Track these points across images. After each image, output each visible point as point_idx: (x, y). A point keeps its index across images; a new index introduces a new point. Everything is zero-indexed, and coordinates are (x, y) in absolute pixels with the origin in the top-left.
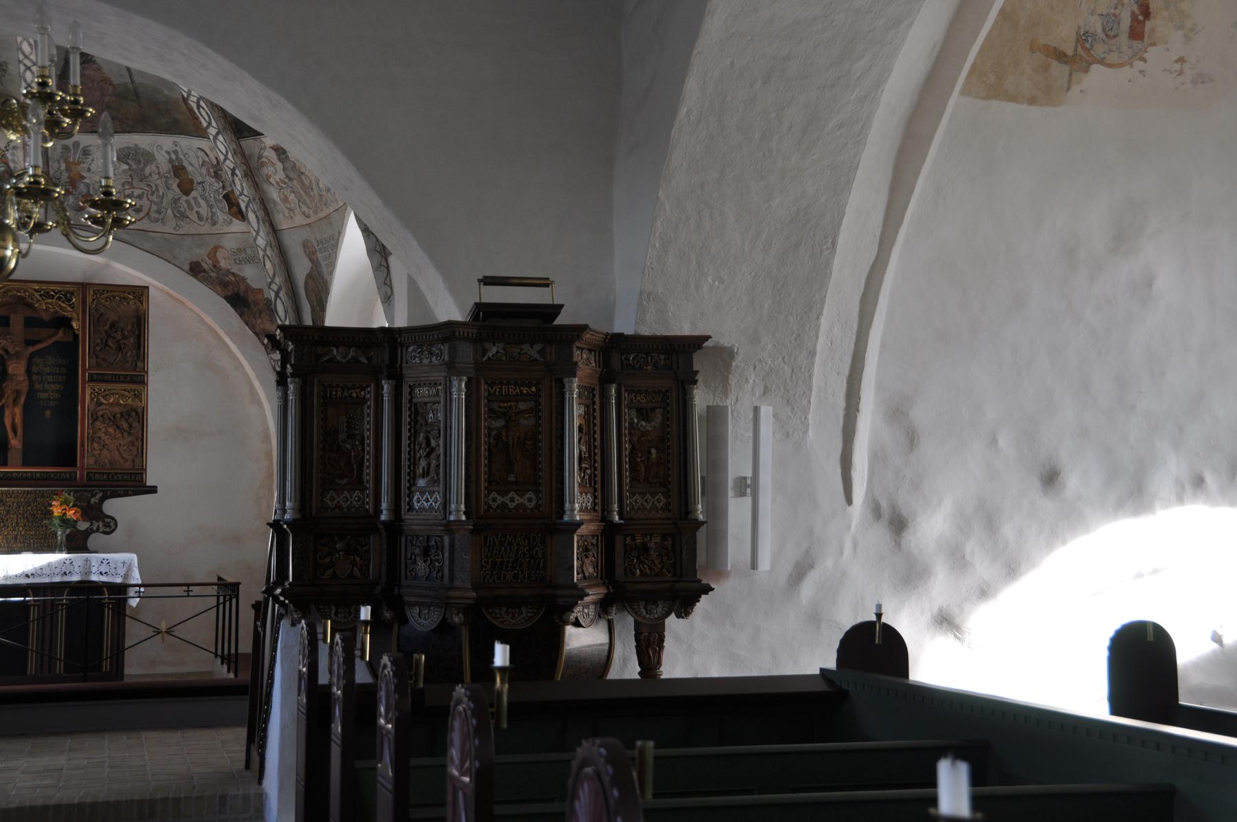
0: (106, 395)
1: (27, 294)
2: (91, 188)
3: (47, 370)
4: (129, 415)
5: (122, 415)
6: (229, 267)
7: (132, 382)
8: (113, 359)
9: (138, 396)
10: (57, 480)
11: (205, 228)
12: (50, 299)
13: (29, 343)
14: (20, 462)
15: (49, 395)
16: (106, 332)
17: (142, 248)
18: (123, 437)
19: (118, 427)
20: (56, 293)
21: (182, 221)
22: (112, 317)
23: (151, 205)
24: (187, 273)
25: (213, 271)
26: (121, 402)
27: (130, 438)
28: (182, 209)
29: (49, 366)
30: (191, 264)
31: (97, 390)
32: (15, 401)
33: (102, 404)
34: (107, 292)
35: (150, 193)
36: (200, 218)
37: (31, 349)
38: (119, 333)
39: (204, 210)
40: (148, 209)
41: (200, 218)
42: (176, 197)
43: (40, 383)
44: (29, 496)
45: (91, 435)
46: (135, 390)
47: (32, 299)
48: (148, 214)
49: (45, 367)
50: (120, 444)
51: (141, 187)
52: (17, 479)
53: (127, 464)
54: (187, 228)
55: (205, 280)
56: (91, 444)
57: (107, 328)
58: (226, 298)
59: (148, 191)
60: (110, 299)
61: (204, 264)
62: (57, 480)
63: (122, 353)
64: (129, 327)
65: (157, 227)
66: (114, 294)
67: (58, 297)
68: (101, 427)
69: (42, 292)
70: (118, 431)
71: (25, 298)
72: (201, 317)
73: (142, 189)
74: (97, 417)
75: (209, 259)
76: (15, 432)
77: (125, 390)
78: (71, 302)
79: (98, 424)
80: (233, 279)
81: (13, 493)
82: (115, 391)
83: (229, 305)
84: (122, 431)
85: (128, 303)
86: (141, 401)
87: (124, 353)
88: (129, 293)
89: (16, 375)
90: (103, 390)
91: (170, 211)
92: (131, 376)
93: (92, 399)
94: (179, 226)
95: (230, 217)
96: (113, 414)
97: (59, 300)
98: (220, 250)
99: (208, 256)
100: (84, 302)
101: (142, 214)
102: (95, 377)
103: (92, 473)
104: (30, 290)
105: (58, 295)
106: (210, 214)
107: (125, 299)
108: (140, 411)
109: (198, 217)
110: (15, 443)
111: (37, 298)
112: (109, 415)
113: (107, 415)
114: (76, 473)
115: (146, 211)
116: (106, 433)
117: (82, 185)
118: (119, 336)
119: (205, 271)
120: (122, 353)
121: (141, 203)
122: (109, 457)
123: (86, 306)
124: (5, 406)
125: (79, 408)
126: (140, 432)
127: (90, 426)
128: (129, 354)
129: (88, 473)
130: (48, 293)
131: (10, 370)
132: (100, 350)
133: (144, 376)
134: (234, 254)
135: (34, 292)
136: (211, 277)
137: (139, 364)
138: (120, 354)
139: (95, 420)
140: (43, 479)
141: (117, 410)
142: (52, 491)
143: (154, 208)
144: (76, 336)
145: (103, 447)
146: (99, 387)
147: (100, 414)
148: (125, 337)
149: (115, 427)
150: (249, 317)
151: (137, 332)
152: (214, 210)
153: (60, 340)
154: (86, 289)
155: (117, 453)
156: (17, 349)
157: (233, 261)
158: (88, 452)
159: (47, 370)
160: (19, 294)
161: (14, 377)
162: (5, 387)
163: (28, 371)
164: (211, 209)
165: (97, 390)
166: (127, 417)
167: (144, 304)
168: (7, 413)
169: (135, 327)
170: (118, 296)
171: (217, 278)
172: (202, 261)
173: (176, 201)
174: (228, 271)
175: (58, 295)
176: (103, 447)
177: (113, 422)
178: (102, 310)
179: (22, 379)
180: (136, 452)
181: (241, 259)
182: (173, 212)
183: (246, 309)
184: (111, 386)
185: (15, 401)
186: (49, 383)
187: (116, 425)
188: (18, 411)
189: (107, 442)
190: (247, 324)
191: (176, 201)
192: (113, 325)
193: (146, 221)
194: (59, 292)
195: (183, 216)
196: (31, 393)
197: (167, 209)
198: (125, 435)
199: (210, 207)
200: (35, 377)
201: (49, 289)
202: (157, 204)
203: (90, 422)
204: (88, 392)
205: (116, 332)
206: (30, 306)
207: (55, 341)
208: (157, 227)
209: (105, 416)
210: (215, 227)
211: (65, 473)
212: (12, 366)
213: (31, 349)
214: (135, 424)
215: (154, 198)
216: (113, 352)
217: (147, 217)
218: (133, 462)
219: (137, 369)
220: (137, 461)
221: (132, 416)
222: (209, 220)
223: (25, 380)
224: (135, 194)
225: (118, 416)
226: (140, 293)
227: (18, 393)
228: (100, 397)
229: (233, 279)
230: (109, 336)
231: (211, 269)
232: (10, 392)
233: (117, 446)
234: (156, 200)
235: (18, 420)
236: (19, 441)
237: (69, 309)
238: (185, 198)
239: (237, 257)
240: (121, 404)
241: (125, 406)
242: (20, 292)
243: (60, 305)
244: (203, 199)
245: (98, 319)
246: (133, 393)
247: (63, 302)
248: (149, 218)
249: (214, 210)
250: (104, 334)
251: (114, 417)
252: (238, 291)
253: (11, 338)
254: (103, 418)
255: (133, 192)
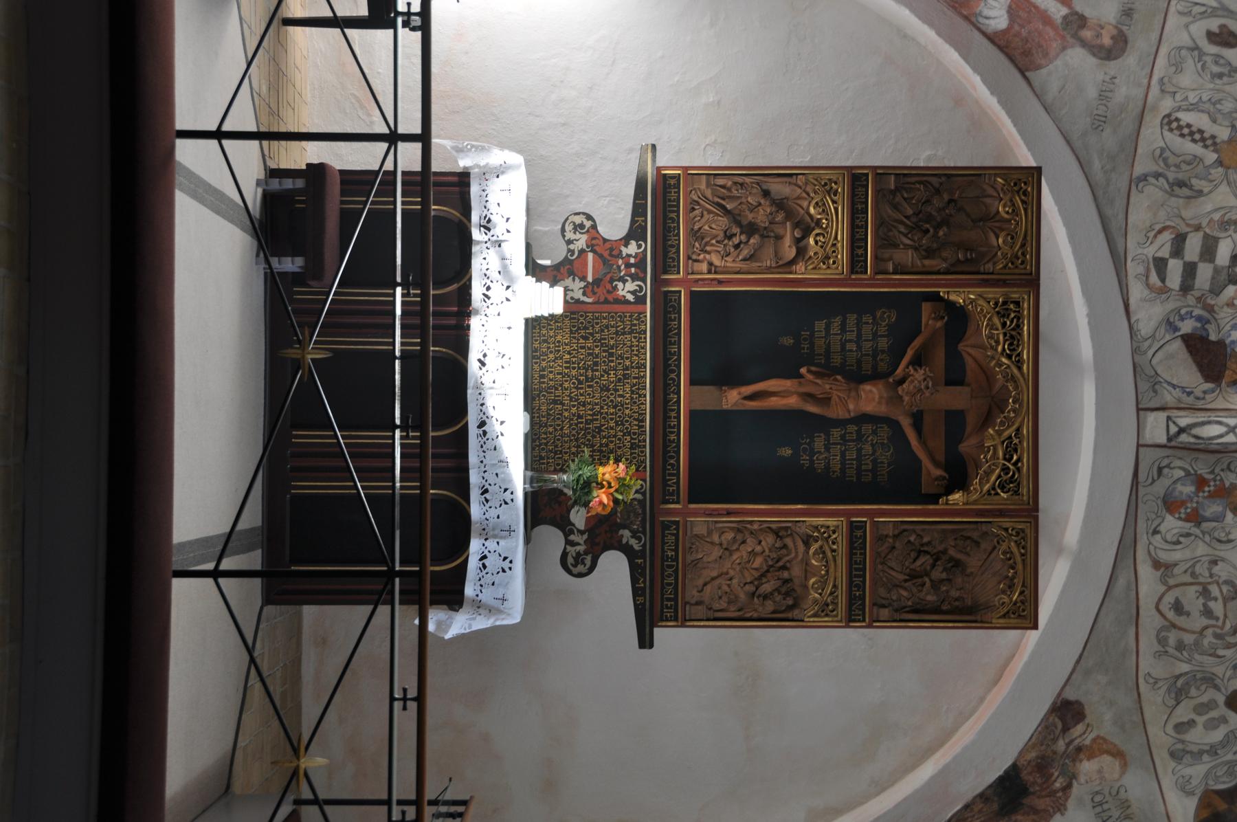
0: (824, 553)
1: (1012, 415)
2: (1214, 524)
3: (868, 449)
4: (787, 594)
5: (786, 581)
6: (1082, 779)
7: (851, 600)
8: (893, 564)
9: (825, 610)
10: (664, 469)
11: (1161, 737)
12: (1005, 455)
13: (918, 419)
14: (698, 406)
15: (820, 452)
16: (945, 552)
17: (1102, 613)
18: (745, 584)
19: (763, 575)
20: (1015, 464)
21: (1169, 691)
22: (973, 562)
23: (1194, 632)
24: (1059, 694)
25: (1068, 745)
26: (813, 580)
27: (742, 596)
28: (1193, 692)
29: (874, 452)
30: (1078, 703)
31: (834, 536)
32: (809, 397)
33: (807, 544)
34: (1023, 555)
35: (1219, 631)
36: (1181, 727)
37: (906, 423)
38: (944, 575)
39: (1199, 736)
40: (1184, 625)
41: (1181, 727)
42: (1218, 681)
43: (843, 437)
44: (636, 423)
45: (748, 526)
46: (836, 604)
47: (1002, 423)
48: (1174, 626)
49: (872, 445)
50: (731, 579)
51: (1230, 615)
52: (666, 401)
53: (695, 592)
54: (1154, 701)
55: (1047, 727)
56: (732, 529)
57: (952, 552)
58: (1014, 766)
59: (1222, 628)
60: (1010, 559)
61: (1080, 728)
62: (664, 469)
63: (906, 581)
64: (954, 593)
65: (1148, 643)
66: (1020, 567)
67: (1008, 468)
68: (763, 543)
69: (1016, 441)
70: (756, 574)
71: (1003, 413)
72: (971, 716)
73: (1226, 616)
74: (781, 538)
75: (1094, 740)
76: (751, 397)
77: (835, 586)
78: (999, 491)
79: (770, 539)
80: (1057, 785)
81: (640, 396)
82: (832, 570)
83: (1001, 773)
84: (756, 583)
85: (1003, 592)
86: (815, 615)
87: (907, 584)
88: (1022, 593)
89: (858, 395)
90: (835, 547)
91: (1185, 667)
92: (863, 598)
93: (816, 528)
94: (1156, 683)
95: (1199, 792)
96: (788, 565)
97: (1003, 470)
98: (1117, 764)
99: (1098, 737)
100: (1001, 513)
101: (1171, 615)
102: (859, 533)
103: (677, 529)
104: (1019, 420)
105: (1011, 467)
106: (1195, 749)
107: (1011, 587)
108: (796, 613)
109: (1183, 723)
110: (732, 398)
111: (1004, 431)
112: (787, 558)
113: (787, 555)
114: (678, 502)
115: (1178, 623)
116: (753, 553)
117: (1220, 509)
118: (938, 574)
119: (1066, 729)
120: (906, 581)
121: (1195, 614)
122: (705, 559)
123: (994, 516)
124: (802, 380)
125: (799, 506)
126: (755, 615)
127: (765, 525)
128: (905, 593)
129: (677, 523)
130: (1016, 450)
131: (867, 387)
132: (909, 541)
133: (864, 621)
134: (1114, 793)
135: (1015, 427)
136: (1055, 740)
137: (885, 613)
138: (902, 577)
139: (777, 533)
140: (665, 446)
141: (796, 571)
142: (644, 462)
143: (1189, 639)
144: (934, 499)
145: (726, 549)
146: (839, 539)
147: (788, 541)
148: (936, 585)
149: (765, 568)
150: (980, 811)
151: (944, 608)
152: (1206, 757)
153: (924, 468)
154: (1025, 517)
155: (715, 574)
156: (906, 399)
157: (1097, 789)
158: (716, 522)
159: (868, 449)
160: (1011, 401)
161: (853, 394)
162: (836, 380)
163: (863, 418)
164: (1207, 752)
165: (834, 536)
166: (783, 590)
167: (1001, 621)
168: (787, 384)
169: (957, 603)
170: (1016, 573)
171: (1055, 753)
172: (1088, 725)
173: (1210, 681)
174: (1074, 776)
175: (1011, 467)
176: (726, 549)
177: (772, 566)
178: (984, 545)
179: (851, 407)
180: (716, 606)
181: (1106, 807)
182: (1186, 673)
183: (995, 806)
184: (842, 561)
185: (809, 397)
186: (843, 454)
187: (768, 571)
188: (792, 402)
189: (735, 557)
190: (967, 807)
191: (1210, 681)
192: (957, 564)
193: (1158, 622)
194: (1018, 469)
195: (1179, 693)
196: (824, 424)
197: (1189, 661)
198: (751, 588)
199: (1213, 751)
200: (852, 428)
201: (1022, 454)
202: (1197, 644)
203: (774, 526)
204: (831, 522)
205: (945, 570)
206: (987, 421)
207: (920, 461)
208: (1148, 643)
209: (784, 551)
210: (1166, 756)
211: (678, 483)
212: (874, 390)
213: (906, 423)
214: (770, 606)
215: (1208, 639)
216: (907, 564)
217: (1167, 623)
218: (698, 603)
219: (875, 609)
220: (700, 611)
221: (784, 599)
222: (1180, 746)
223: (849, 412)
224: (1211, 604)
225: (786, 575)
227: (825, 401)
228: (820, 543)
229: (1057, 785)
230: (937, 558)
231: (1072, 741)
232: (827, 387)
233: (727, 573)
234: (1206, 642)
235: (774, 403)
236: (735, 404)
237: (987, 487)
238: (1221, 699)
239: (1108, 798)
240: (806, 579)
241: (806, 587)
242: (1013, 402)
243: (994, 471)
244: (1227, 735)
245: (969, 538)
246: (829, 600)
247: (999, 476)
248: (1162, 629)
249: (1206, 757)
250: (941, 548)
251: (784, 568)
252: (1033, 793)
253: (927, 388)
254: (781, 548)
255: (1216, 599)
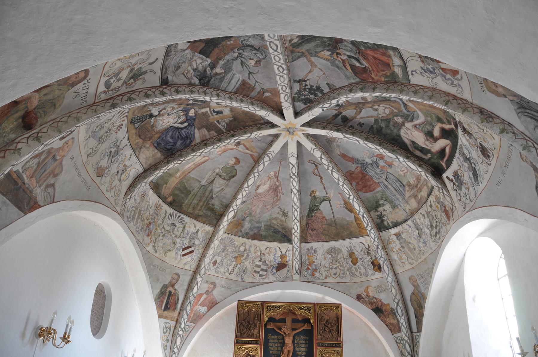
3: (300, 342)
6: (374, 295)
8: (327, 336)
11: (363, 279)
13: (294, 330)
15: (301, 353)
16: (324, 324)
20: (304, 308)
22: (327, 318)
25: (366, 298)
28: (353, 272)
30: (357, 295)
36: (361, 275)
37: (294, 332)
38: (330, 324)
39: (362, 271)
41: (361, 275)
43: (298, 347)
46: (337, 350)
54: (355, 280)
57: (324, 322)
58: (372, 310)
61: (362, 295)
64: (334, 322)
65: (343, 280)
66: (327, 307)
69: (299, 307)
75: (365, 292)
77: (333, 350)
80: (375, 300)
82: (329, 351)
83: (374, 313)
85: (333, 311)
88: (333, 307)
89: (288, 343)
91: (348, 273)
92: (336, 344)
95: (374, 272)
98: (370, 288)
100: (315, 311)
101: (337, 276)
106: (365, 272)
118: (329, 326)
119: (363, 298)
121: (336, 271)
128: (334, 334)
131: (286, 341)
136: (366, 301)
143: (342, 272)
144: (312, 326)
148: (332, 326)
152: (367, 270)
156: (289, 332)
159: (300, 342)
161: (287, 345)
171: (368, 301)
173: (350, 268)
174: (373, 297)
178: (323, 315)
179: (290, 345)
183: (381, 314)
186: (302, 348)
190: (382, 321)
191: (350, 268)
192: (327, 321)
193: (338, 278)
194: (305, 307)
195: (354, 274)
197: (347, 272)
199: (365, 268)
200: (295, 345)
202: (343, 271)
204: (318, 351)
205: (328, 324)
208: (343, 280)
213: (294, 332)
215: (342, 268)
222: (365, 275)
224: (334, 267)
226: (338, 307)
227: (289, 351)
228: (323, 354)
229: (375, 300)
230: (326, 326)
238: (354, 266)
248: (340, 277)
249: (367, 270)
250: (323, 325)
